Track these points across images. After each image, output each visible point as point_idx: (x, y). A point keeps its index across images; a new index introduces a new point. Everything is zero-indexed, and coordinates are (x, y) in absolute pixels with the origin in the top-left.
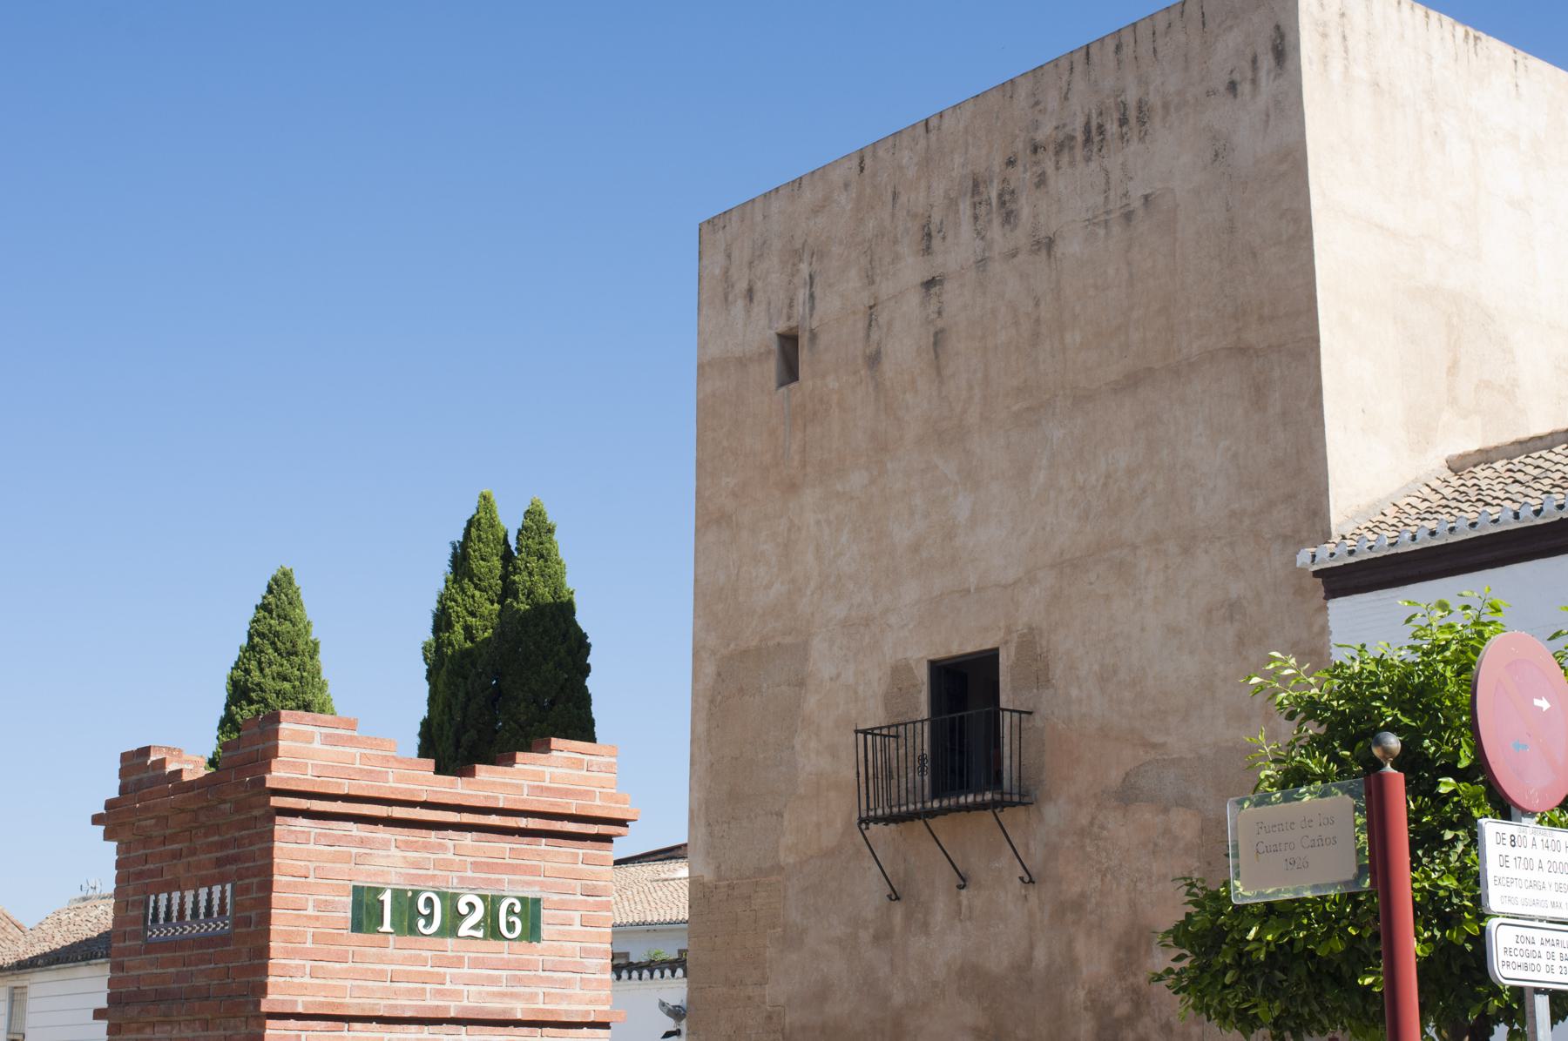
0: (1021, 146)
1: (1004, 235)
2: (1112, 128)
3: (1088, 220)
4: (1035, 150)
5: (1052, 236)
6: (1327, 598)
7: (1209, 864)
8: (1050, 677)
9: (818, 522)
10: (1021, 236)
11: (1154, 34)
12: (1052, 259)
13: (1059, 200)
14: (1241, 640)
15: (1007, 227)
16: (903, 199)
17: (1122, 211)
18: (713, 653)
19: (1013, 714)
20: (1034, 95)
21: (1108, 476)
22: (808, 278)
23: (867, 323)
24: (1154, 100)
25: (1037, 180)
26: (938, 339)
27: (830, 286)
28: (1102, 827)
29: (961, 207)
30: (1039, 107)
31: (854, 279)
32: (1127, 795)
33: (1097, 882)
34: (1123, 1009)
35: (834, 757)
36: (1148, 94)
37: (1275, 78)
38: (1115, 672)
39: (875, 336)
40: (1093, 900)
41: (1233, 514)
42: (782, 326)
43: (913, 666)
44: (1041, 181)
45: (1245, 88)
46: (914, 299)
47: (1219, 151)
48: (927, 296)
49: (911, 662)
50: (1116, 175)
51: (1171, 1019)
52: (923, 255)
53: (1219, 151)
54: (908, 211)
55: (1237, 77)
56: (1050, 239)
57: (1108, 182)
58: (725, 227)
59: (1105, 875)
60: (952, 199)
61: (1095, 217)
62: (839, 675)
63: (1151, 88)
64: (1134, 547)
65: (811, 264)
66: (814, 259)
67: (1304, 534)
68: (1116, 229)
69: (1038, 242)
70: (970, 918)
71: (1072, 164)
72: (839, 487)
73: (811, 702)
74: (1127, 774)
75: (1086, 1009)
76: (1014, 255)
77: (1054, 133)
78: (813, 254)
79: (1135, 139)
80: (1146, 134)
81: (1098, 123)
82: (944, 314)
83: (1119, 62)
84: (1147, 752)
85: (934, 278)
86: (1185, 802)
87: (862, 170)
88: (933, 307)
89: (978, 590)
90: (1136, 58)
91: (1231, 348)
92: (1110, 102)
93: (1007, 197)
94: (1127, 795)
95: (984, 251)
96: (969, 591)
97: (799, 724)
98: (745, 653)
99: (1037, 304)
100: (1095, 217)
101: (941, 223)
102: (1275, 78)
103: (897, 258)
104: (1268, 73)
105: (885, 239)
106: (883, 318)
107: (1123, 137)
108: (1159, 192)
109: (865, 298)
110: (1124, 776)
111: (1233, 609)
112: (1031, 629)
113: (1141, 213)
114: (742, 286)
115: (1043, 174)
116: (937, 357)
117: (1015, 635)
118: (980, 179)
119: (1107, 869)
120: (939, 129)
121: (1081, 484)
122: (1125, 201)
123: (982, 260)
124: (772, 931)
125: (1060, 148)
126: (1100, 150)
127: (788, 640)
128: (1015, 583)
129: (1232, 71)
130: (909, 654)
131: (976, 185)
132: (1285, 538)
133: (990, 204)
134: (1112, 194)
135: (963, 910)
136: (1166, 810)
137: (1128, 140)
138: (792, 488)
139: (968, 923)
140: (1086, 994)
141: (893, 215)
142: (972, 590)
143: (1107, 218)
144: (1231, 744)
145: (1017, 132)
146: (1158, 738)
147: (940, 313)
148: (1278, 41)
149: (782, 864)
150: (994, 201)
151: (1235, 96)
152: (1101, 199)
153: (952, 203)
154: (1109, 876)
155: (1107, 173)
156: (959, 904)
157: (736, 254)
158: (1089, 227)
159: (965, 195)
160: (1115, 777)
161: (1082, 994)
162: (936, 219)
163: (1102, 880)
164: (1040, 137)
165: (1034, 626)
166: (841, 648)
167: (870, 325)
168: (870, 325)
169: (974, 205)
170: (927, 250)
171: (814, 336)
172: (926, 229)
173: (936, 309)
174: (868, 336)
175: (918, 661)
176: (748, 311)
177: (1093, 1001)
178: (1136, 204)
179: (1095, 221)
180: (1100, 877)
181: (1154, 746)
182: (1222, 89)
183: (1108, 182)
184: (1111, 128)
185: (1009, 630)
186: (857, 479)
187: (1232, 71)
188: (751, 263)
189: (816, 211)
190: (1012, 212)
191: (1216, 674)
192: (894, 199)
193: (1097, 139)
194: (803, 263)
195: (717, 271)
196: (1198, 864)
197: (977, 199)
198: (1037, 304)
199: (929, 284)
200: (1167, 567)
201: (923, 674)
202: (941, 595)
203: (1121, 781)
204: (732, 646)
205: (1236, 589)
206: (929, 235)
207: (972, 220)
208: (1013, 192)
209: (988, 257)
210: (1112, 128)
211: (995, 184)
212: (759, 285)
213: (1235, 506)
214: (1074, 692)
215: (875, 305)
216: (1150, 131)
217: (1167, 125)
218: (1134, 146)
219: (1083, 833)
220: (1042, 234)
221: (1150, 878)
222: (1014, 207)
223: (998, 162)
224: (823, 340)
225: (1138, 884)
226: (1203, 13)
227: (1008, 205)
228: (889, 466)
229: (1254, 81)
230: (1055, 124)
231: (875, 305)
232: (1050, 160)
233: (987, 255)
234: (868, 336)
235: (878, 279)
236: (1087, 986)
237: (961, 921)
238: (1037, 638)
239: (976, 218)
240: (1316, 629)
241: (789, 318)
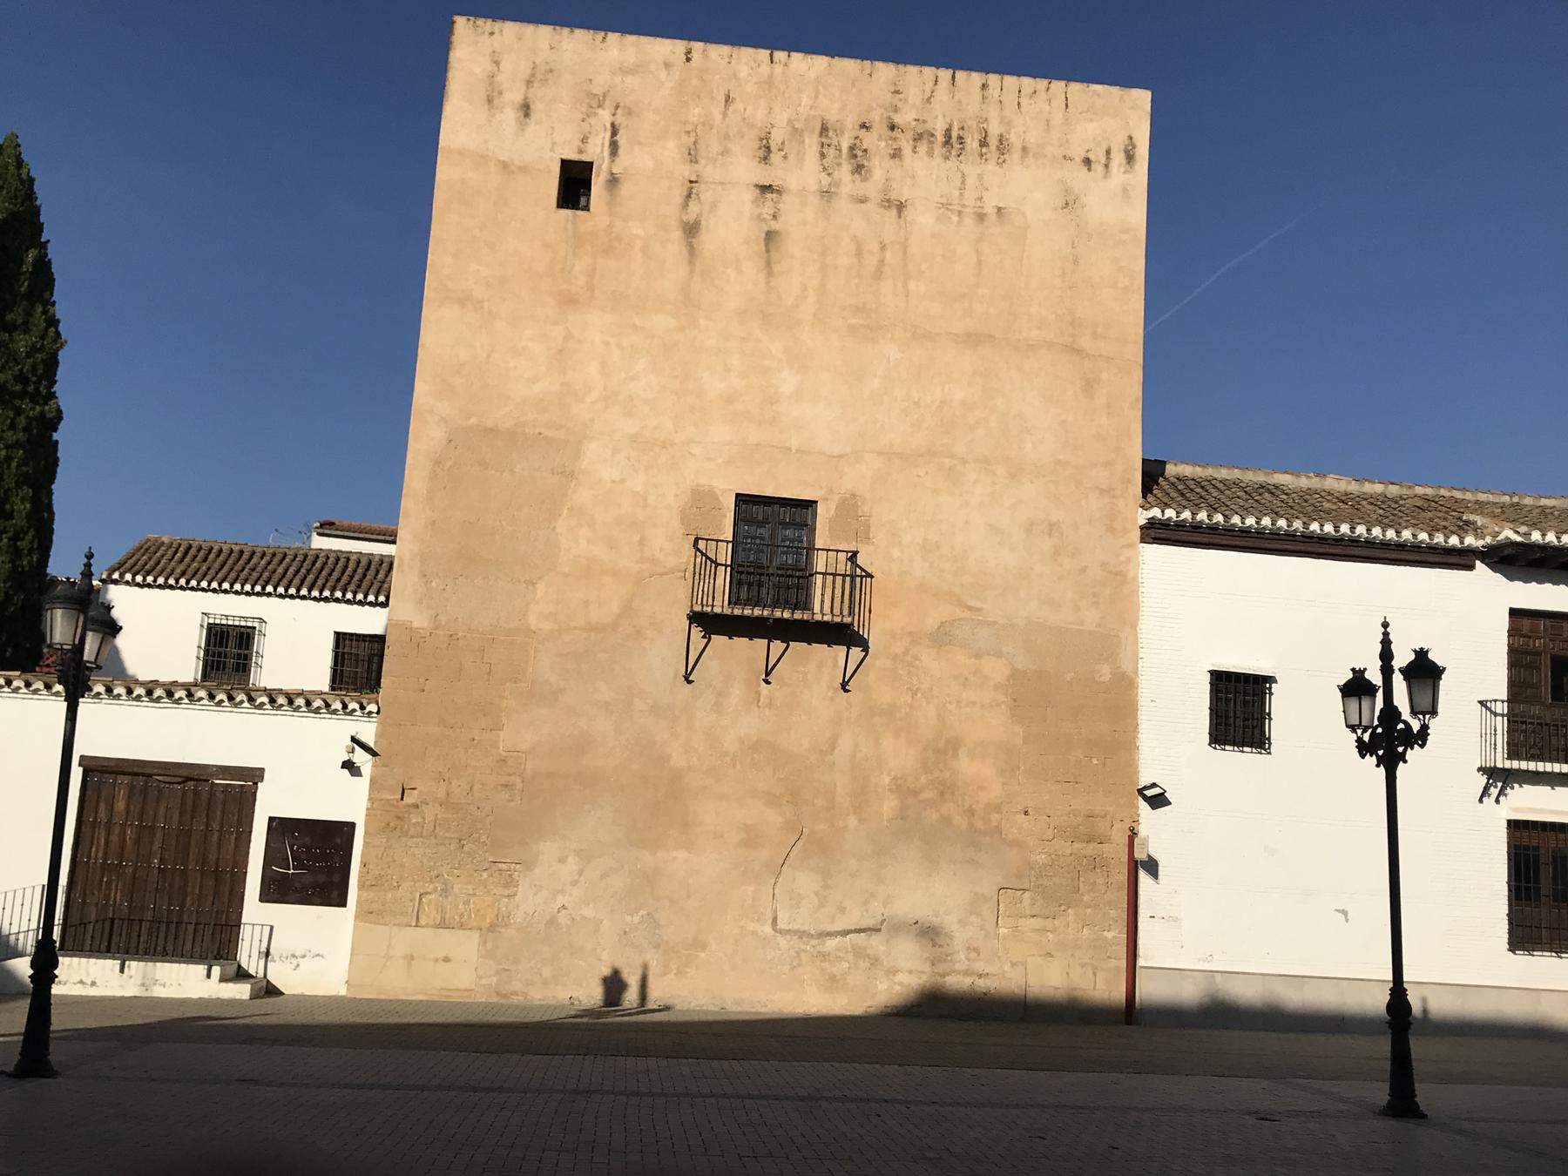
0: (877, 118)
1: (854, 182)
2: (972, 143)
3: (942, 204)
4: (892, 127)
5: (903, 201)
6: (1141, 542)
7: (1015, 700)
8: (871, 536)
9: (607, 344)
10: (872, 188)
11: (1020, 91)
12: (902, 219)
13: (914, 176)
14: (1057, 552)
15: (857, 176)
16: (738, 105)
17: (976, 209)
18: (444, 420)
19: (719, 543)
20: (895, 84)
21: (943, 402)
22: (609, 126)
23: (685, 193)
24: (1013, 138)
25: (892, 152)
26: (770, 237)
27: (640, 144)
28: (916, 658)
29: (807, 141)
30: (900, 96)
31: (671, 150)
32: (941, 638)
33: (908, 697)
34: (928, 794)
35: (611, 548)
36: (1009, 134)
37: (1124, 172)
38: (938, 548)
39: (694, 207)
40: (903, 711)
41: (1058, 462)
42: (572, 155)
43: (719, 492)
44: (896, 155)
45: (1098, 168)
46: (749, 195)
47: (1070, 203)
48: (762, 197)
49: (716, 490)
50: (971, 181)
51: (974, 806)
52: (760, 162)
53: (1070, 203)
54: (744, 119)
55: (1092, 157)
56: (902, 203)
57: (963, 182)
58: (492, 34)
59: (914, 694)
60: (797, 129)
61: (950, 204)
62: (623, 481)
63: (1013, 130)
64: (964, 461)
65: (614, 115)
66: (619, 111)
67: (1118, 492)
68: (969, 221)
69: (888, 201)
70: (770, 706)
71: (930, 154)
72: (637, 321)
73: (582, 496)
74: (942, 623)
75: (889, 790)
76: (862, 202)
77: (914, 123)
78: (617, 107)
79: (994, 163)
80: (1004, 161)
81: (959, 135)
82: (782, 219)
83: (984, 98)
84: (963, 611)
85: (770, 186)
86: (998, 654)
87: (688, 60)
88: (767, 209)
89: (797, 451)
90: (1001, 102)
91: (1066, 346)
92: (973, 124)
93: (859, 153)
94: (941, 638)
95: (830, 185)
96: (790, 449)
97: (565, 511)
98: (493, 431)
99: (883, 248)
100: (950, 204)
101: (783, 143)
102: (1124, 172)
103: (725, 152)
104: (1120, 166)
105: (714, 131)
106: (707, 196)
107: (982, 156)
108: (1010, 210)
109: (687, 171)
110: (939, 624)
111: (1052, 528)
112: (854, 495)
113: (993, 218)
114: (514, 96)
115: (900, 149)
116: (768, 251)
117: (837, 497)
118: (829, 125)
119: (918, 689)
120: (786, 65)
121: (916, 400)
122: (978, 204)
123: (826, 192)
124: (514, 685)
125: (918, 138)
126: (959, 156)
127: (552, 434)
128: (841, 456)
129: (1088, 151)
130: (715, 484)
131: (824, 130)
132: (1102, 491)
133: (840, 151)
134: (966, 194)
135: (762, 699)
136: (978, 656)
137: (986, 160)
138: (570, 301)
139: (767, 710)
140: (892, 780)
141: (725, 115)
142: (794, 451)
143: (962, 209)
144: (1041, 621)
145: (874, 105)
146: (978, 605)
147: (774, 217)
148: (1130, 148)
149: (533, 628)
150: (845, 150)
151: (1089, 170)
152: (957, 193)
153: (797, 133)
154: (919, 695)
155: (963, 175)
156: (758, 693)
157: (507, 65)
158: (942, 210)
159: (813, 131)
160: (931, 622)
161: (886, 779)
162: (776, 138)
163: (913, 697)
164: (897, 119)
165: (857, 494)
166: (629, 459)
167: (689, 196)
168: (689, 196)
169: (823, 144)
170: (765, 159)
171: (613, 181)
172: (765, 142)
173: (772, 212)
174: (685, 206)
175: (725, 491)
176: (522, 126)
177: (898, 786)
178: (990, 210)
179: (948, 206)
180: (910, 694)
181: (971, 608)
182: (1079, 159)
183: (963, 182)
184: (972, 144)
185: (831, 491)
186: (662, 322)
187: (1088, 151)
188: (529, 83)
189: (624, 71)
190: (863, 166)
191: (1032, 569)
192: (727, 101)
193: (957, 146)
194: (604, 109)
195: (478, 70)
196: (1005, 699)
197: (824, 140)
198: (883, 248)
199: (765, 189)
200: (994, 483)
201: (730, 503)
202: (757, 445)
203: (936, 627)
204: (474, 421)
205: (1055, 515)
206: (768, 149)
207: (818, 155)
208: (865, 151)
209: (835, 193)
210: (972, 143)
211: (846, 135)
212: (537, 107)
213: (1061, 457)
214: (896, 553)
215: (696, 182)
216: (1008, 161)
217: (1024, 164)
218: (991, 166)
219: (895, 657)
220: (893, 196)
221: (959, 702)
222: (866, 164)
223: (851, 123)
224: (625, 189)
225: (948, 705)
226: (1066, 97)
227: (859, 159)
228: (702, 322)
229: (1107, 166)
230: (914, 116)
231: (696, 182)
232: (908, 142)
233: (833, 190)
234: (685, 206)
235: (702, 162)
236: (893, 774)
237: (759, 707)
238: (860, 504)
239: (823, 155)
240: (1122, 558)
241: (581, 152)
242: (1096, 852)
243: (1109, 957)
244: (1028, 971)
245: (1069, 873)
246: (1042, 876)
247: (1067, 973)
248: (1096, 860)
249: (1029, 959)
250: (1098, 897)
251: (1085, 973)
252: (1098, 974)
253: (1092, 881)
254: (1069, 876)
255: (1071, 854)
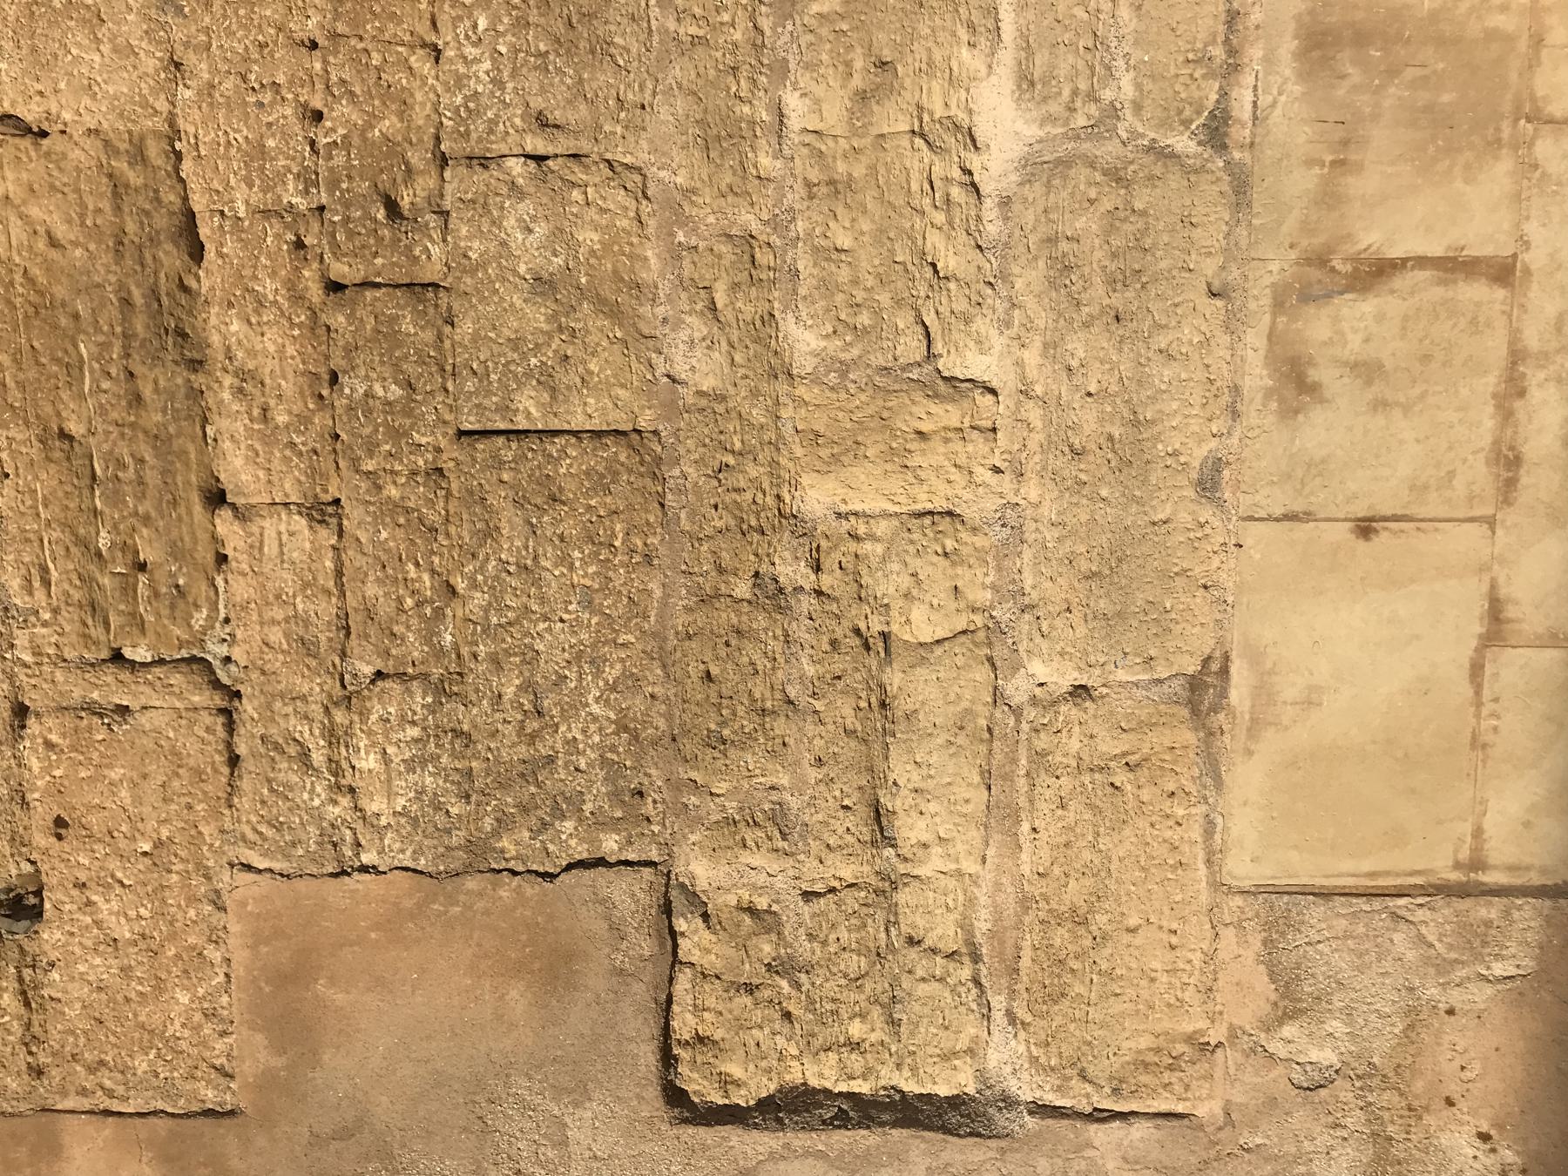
242: (268, 287)
243: (1216, 132)
244: (1345, 869)
245: (490, 533)
246: (532, 770)
247: (1365, 528)
248: (340, 270)
249: (1242, 868)
250: (675, 254)
251: (1366, 370)
252: (1373, 237)
253: (538, 317)
254: (512, 542)
255: (323, 512)
